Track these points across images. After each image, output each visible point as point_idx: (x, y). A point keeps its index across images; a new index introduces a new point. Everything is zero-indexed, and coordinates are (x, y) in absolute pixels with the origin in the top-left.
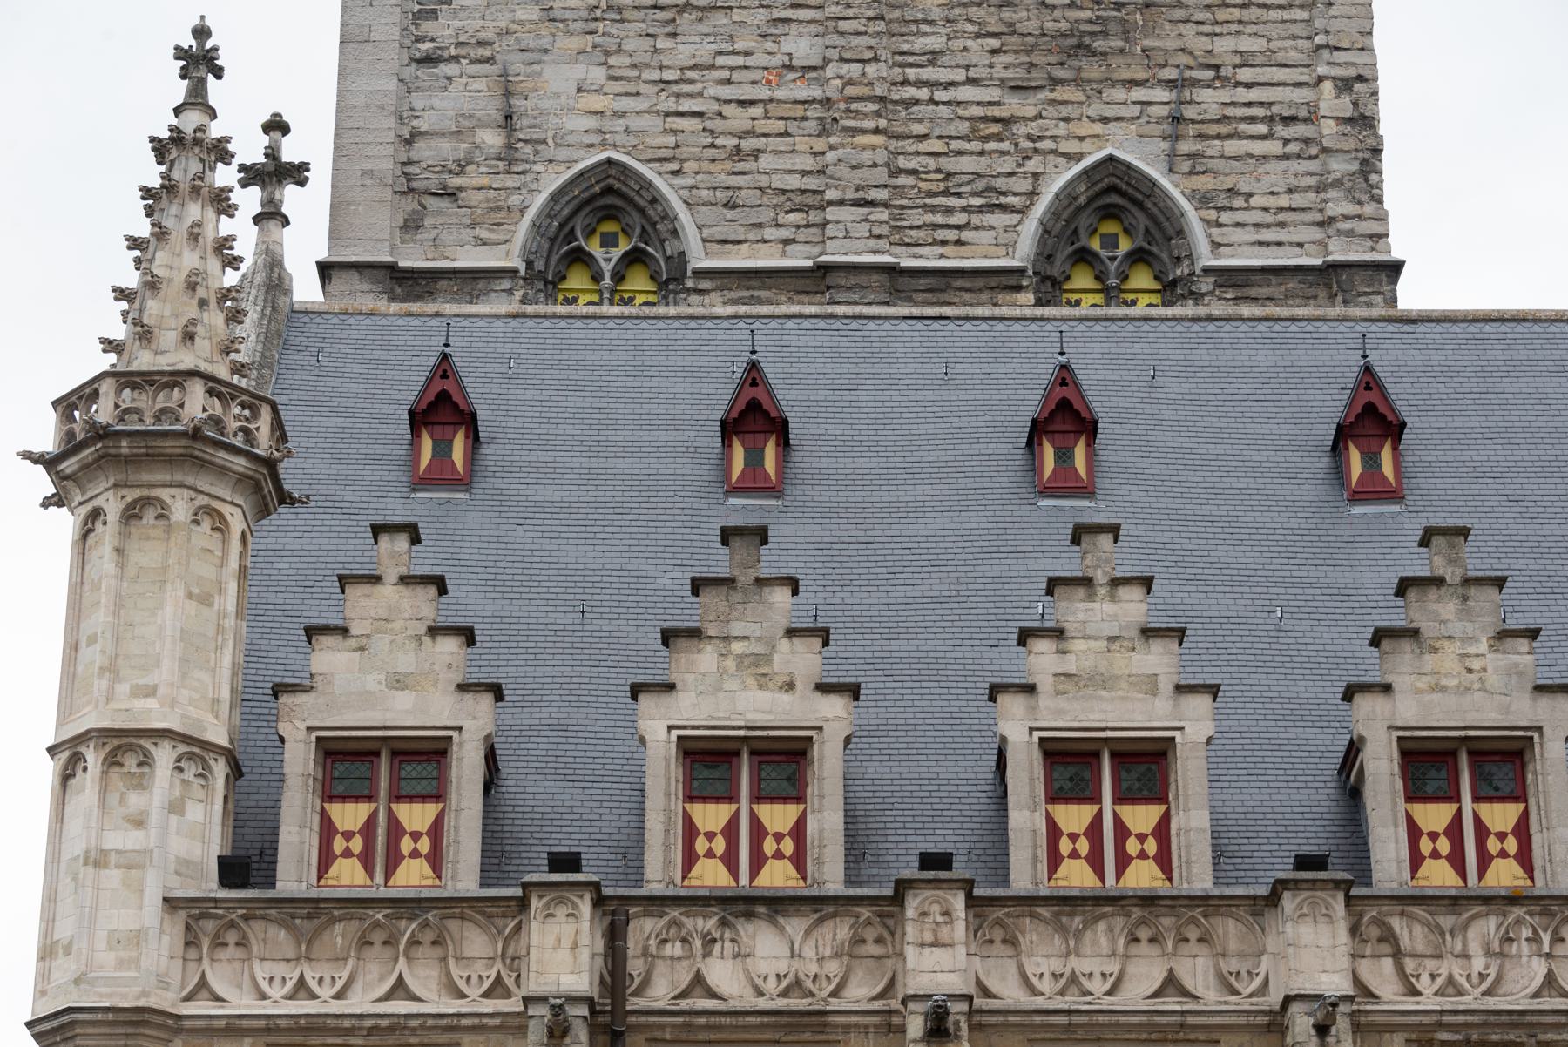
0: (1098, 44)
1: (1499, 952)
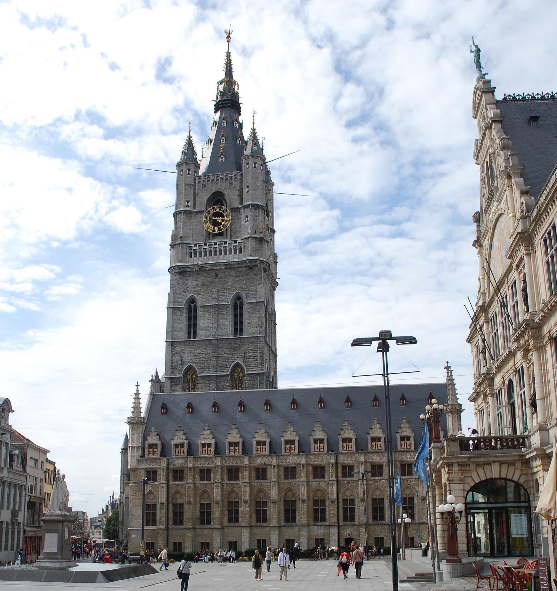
0: (237, 349)
1: (233, 460)
